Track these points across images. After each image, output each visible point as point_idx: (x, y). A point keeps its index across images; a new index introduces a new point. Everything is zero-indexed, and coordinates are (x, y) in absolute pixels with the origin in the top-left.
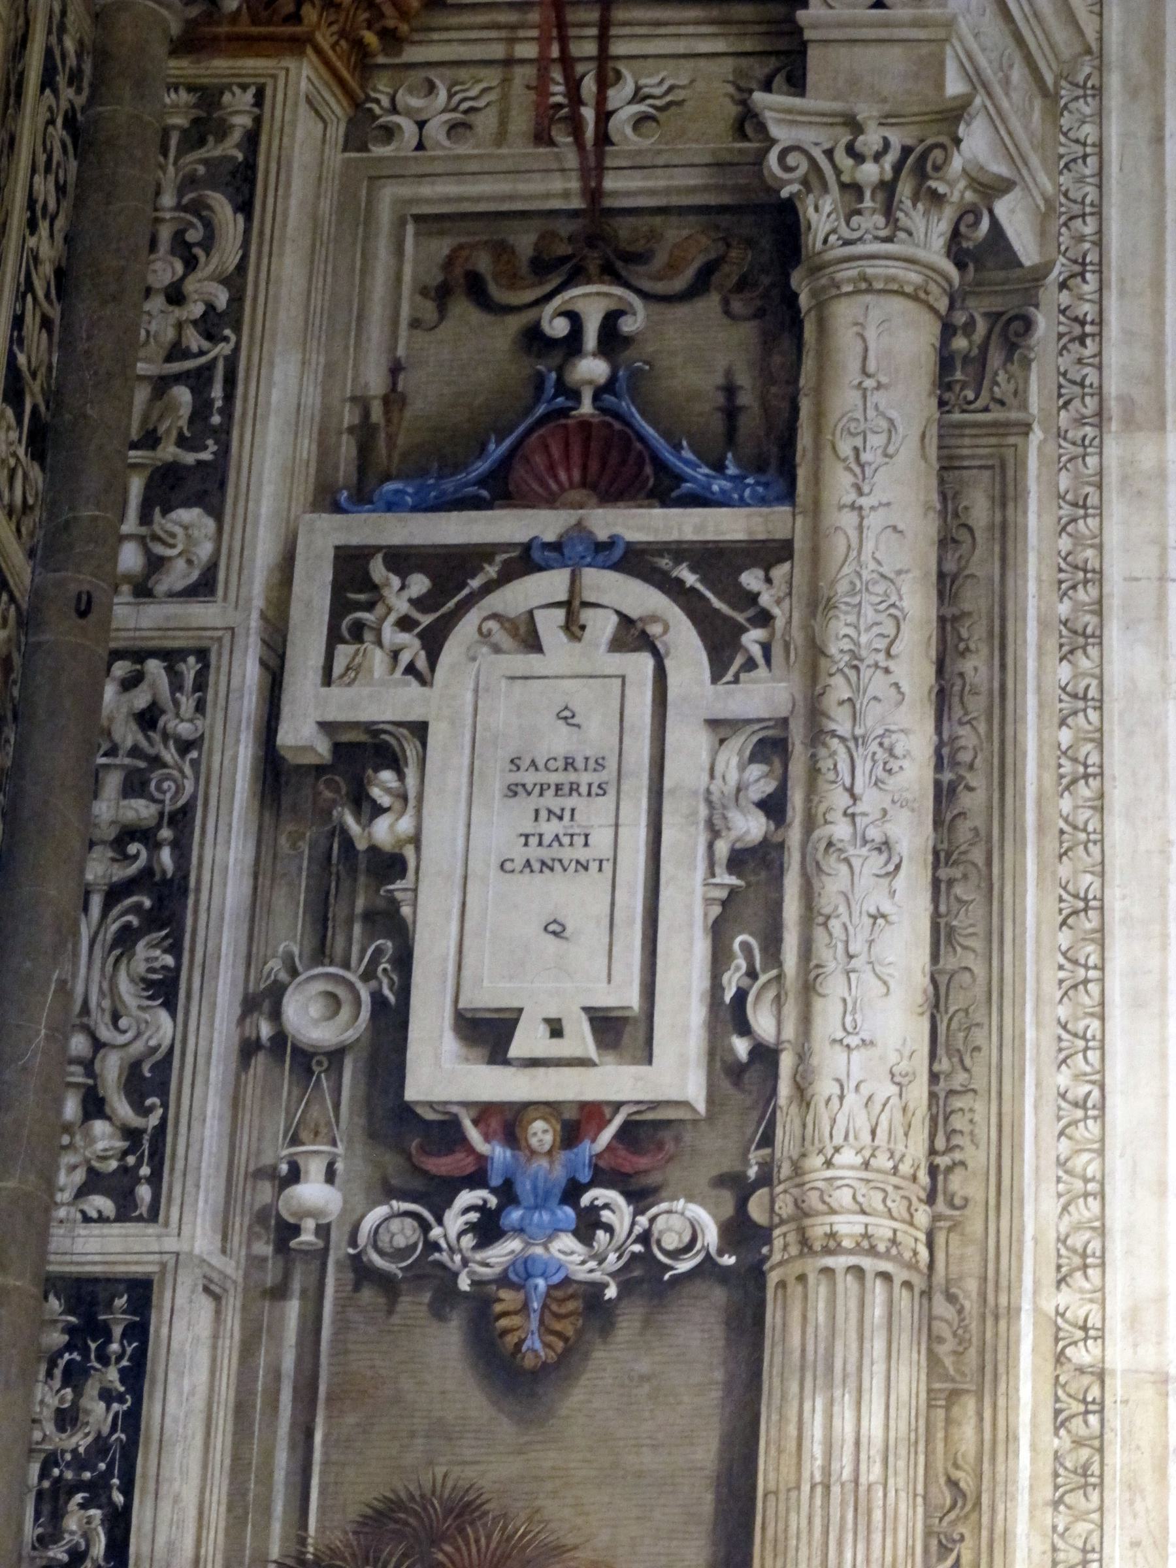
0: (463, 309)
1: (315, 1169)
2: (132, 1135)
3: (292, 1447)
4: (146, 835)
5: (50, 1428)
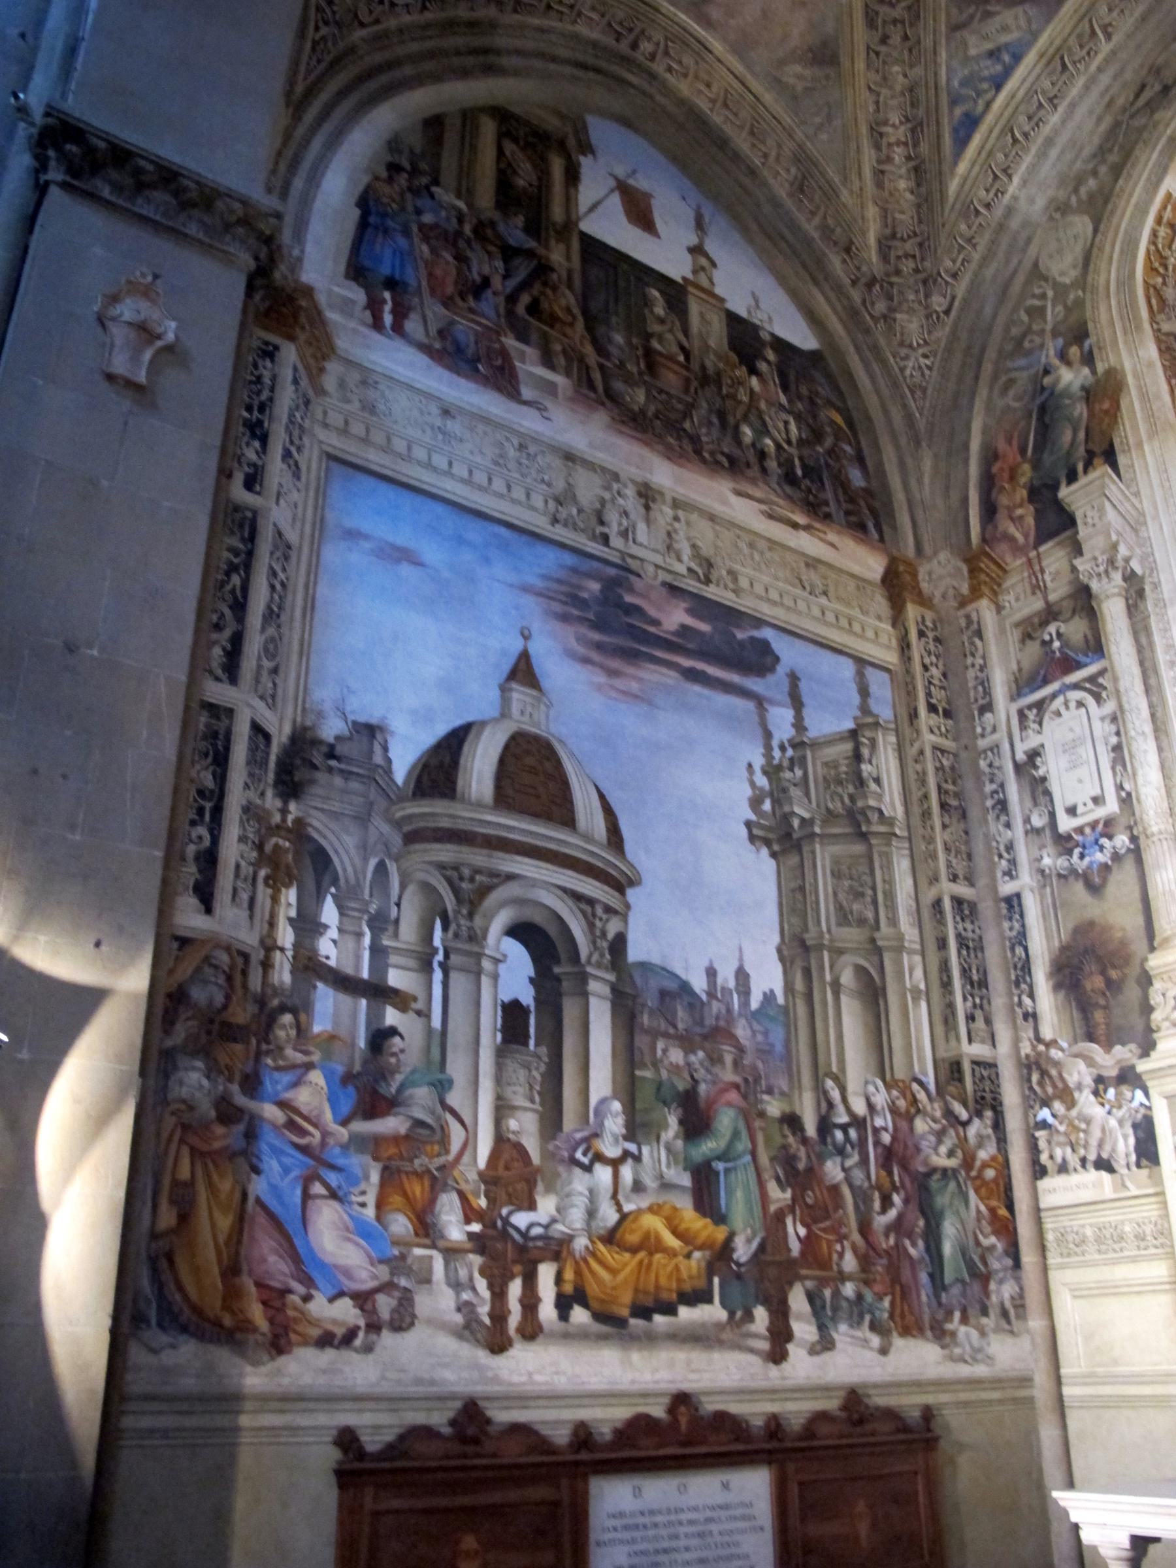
0: (1029, 643)
4: (996, 792)
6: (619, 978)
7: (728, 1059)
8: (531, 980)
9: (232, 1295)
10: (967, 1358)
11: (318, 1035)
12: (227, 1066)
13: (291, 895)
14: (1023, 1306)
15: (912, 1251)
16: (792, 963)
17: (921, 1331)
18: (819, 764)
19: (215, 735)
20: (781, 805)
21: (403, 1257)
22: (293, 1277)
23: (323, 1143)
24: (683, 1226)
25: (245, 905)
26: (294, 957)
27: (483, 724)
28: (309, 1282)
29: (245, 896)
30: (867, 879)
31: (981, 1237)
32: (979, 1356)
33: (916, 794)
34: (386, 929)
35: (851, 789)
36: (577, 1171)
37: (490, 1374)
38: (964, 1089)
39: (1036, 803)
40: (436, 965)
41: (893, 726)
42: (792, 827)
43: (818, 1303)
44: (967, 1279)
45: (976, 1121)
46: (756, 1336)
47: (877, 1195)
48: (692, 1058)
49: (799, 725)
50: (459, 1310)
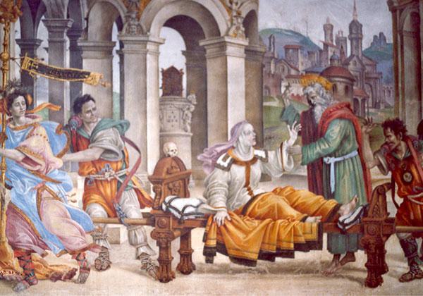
6: (250, 43)
8: (184, 53)
11: (40, 106)
16: (401, 11)
22: (35, 244)
24: (300, 201)
28: (45, 246)
34: (80, 36)
40: (114, 52)
43: (411, 248)
50: (138, 258)
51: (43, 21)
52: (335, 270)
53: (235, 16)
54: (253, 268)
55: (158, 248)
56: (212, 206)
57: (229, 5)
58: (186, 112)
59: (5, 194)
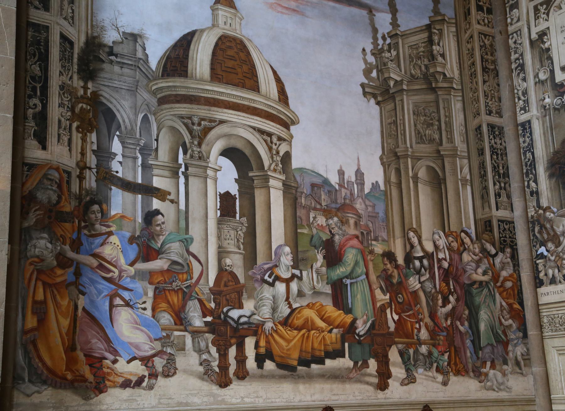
1: (547, 97)
2: (524, 101)
3: (551, 136)
4: (518, 59)
5: (522, 144)
6: (286, 178)
7: (352, 221)
8: (236, 180)
9: (71, 361)
10: (495, 387)
12: (61, 236)
13: (93, 137)
14: (529, 359)
15: (461, 328)
16: (389, 165)
17: (467, 372)
18: (406, 46)
19: (38, 43)
20: (383, 73)
21: (168, 336)
22: (106, 351)
23: (120, 277)
24: (327, 315)
25: (66, 144)
26: (97, 172)
27: (202, 31)
28: (115, 352)
29: (66, 139)
30: (435, 115)
31: (503, 320)
32: (502, 387)
33: (467, 63)
35: (426, 62)
36: (266, 286)
37: (220, 399)
38: (494, 238)
39: (542, 66)
41: (454, 21)
42: (389, 86)
43: (406, 357)
44: (495, 344)
45: (501, 255)
46: (370, 375)
47: (440, 296)
48: (331, 222)
49: (394, 23)
50: (201, 364)
51: (118, 136)
52: (355, 374)
53: (275, 155)
54: (294, 374)
55: (217, 354)
56: (261, 317)
57: (270, 144)
58: (239, 232)
59: (78, 299)
